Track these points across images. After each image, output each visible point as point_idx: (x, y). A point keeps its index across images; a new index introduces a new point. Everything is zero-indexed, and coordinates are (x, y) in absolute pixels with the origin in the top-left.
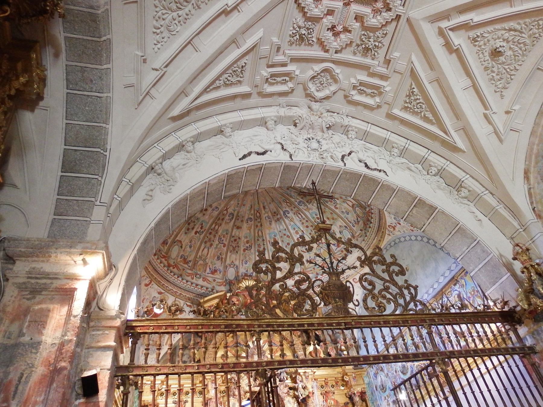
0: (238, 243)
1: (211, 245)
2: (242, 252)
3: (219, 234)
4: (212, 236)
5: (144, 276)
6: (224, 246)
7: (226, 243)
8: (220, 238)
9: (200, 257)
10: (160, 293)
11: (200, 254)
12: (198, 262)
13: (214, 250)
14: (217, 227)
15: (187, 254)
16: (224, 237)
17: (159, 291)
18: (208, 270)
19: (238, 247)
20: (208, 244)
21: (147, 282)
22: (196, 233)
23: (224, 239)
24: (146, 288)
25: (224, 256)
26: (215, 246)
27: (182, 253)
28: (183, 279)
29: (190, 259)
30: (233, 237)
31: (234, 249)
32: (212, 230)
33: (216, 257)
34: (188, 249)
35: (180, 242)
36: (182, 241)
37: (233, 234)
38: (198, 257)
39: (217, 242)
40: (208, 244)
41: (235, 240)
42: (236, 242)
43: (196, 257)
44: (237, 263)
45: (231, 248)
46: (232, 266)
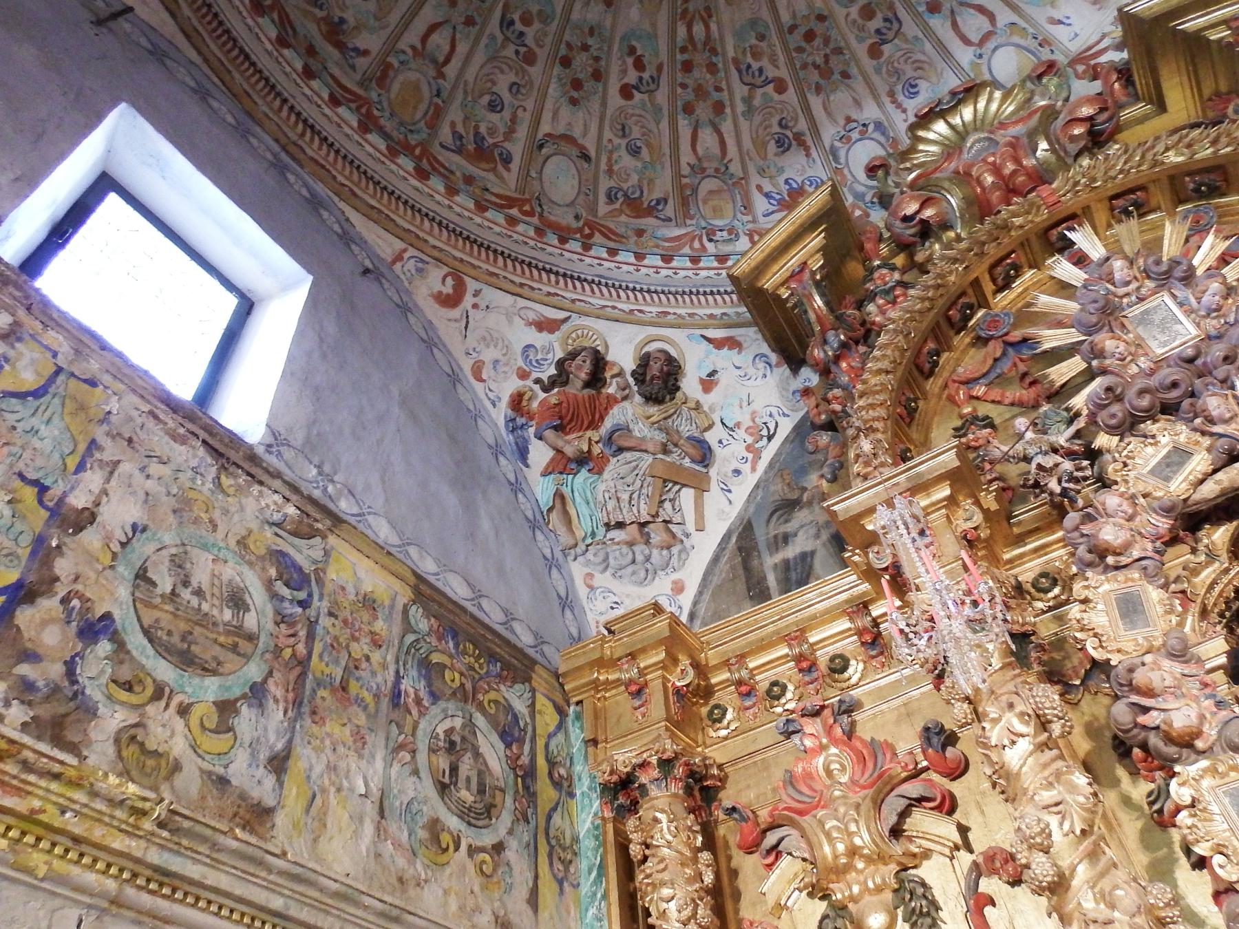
0: (827, 41)
1: (719, 108)
2: (868, 63)
3: (731, 53)
4: (700, 74)
5: (399, 258)
6: (781, 87)
7: (783, 73)
8: (743, 70)
9: (698, 170)
10: (545, 326)
11: (686, 157)
12: (695, 190)
13: (744, 125)
14: (698, 29)
15: (635, 178)
16: (756, 55)
17: (532, 316)
18: (761, 204)
19: (838, 51)
20: (703, 111)
21: (436, 280)
22: (626, 92)
23: (765, 62)
24: (456, 313)
25: (802, 125)
26: (740, 108)
27: (605, 184)
28: (640, 256)
29: (657, 194)
30: (792, 29)
31: (826, 73)
32: (683, 50)
33: (772, 147)
34: (627, 161)
35: (568, 139)
36: (577, 133)
37: (786, 18)
38: (686, 170)
39: (740, 91)
40: (703, 111)
41: (810, 36)
42: (818, 42)
43: (678, 175)
44: (870, 112)
45: (815, 76)
46: (855, 135)
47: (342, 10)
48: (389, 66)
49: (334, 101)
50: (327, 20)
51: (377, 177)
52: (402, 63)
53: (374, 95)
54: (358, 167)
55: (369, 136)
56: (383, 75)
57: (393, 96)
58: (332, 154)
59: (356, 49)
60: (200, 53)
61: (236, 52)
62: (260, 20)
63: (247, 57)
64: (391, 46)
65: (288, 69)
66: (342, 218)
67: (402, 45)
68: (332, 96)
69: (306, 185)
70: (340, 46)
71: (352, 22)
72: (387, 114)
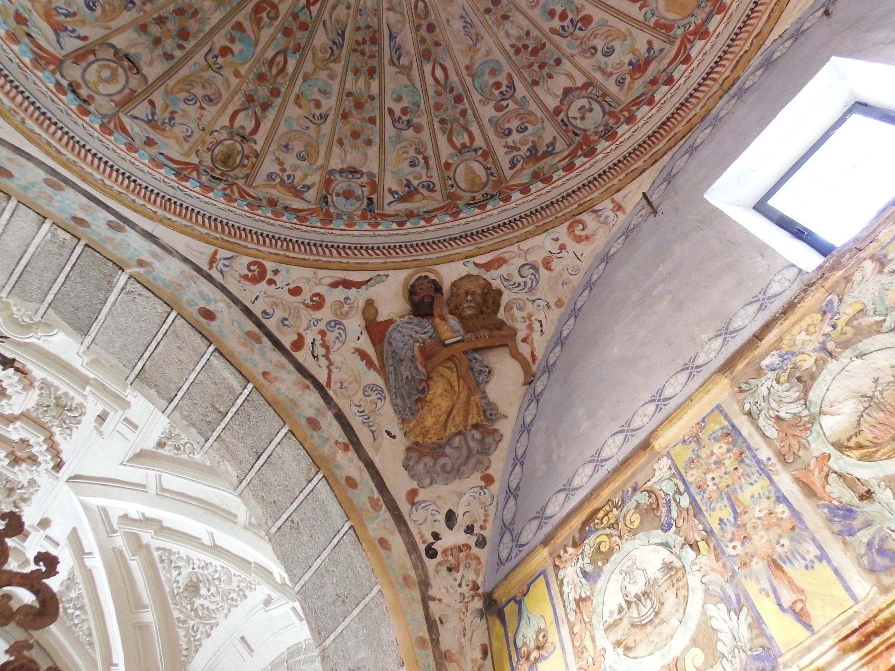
47: (624, 64)
48: (657, 24)
49: (687, 60)
50: (632, 74)
51: (744, 18)
52: (653, 15)
53: (679, 32)
54: (736, 34)
55: (711, 29)
56: (664, 27)
57: (678, 17)
58: (727, 56)
59: (648, 51)
60: (665, 153)
61: (662, 131)
62: (639, 117)
63: (664, 123)
64: (642, 25)
65: (669, 95)
66: (780, 41)
67: (640, 17)
68: (683, 62)
69: (753, 73)
70: (648, 62)
71: (631, 56)
72: (693, 19)
